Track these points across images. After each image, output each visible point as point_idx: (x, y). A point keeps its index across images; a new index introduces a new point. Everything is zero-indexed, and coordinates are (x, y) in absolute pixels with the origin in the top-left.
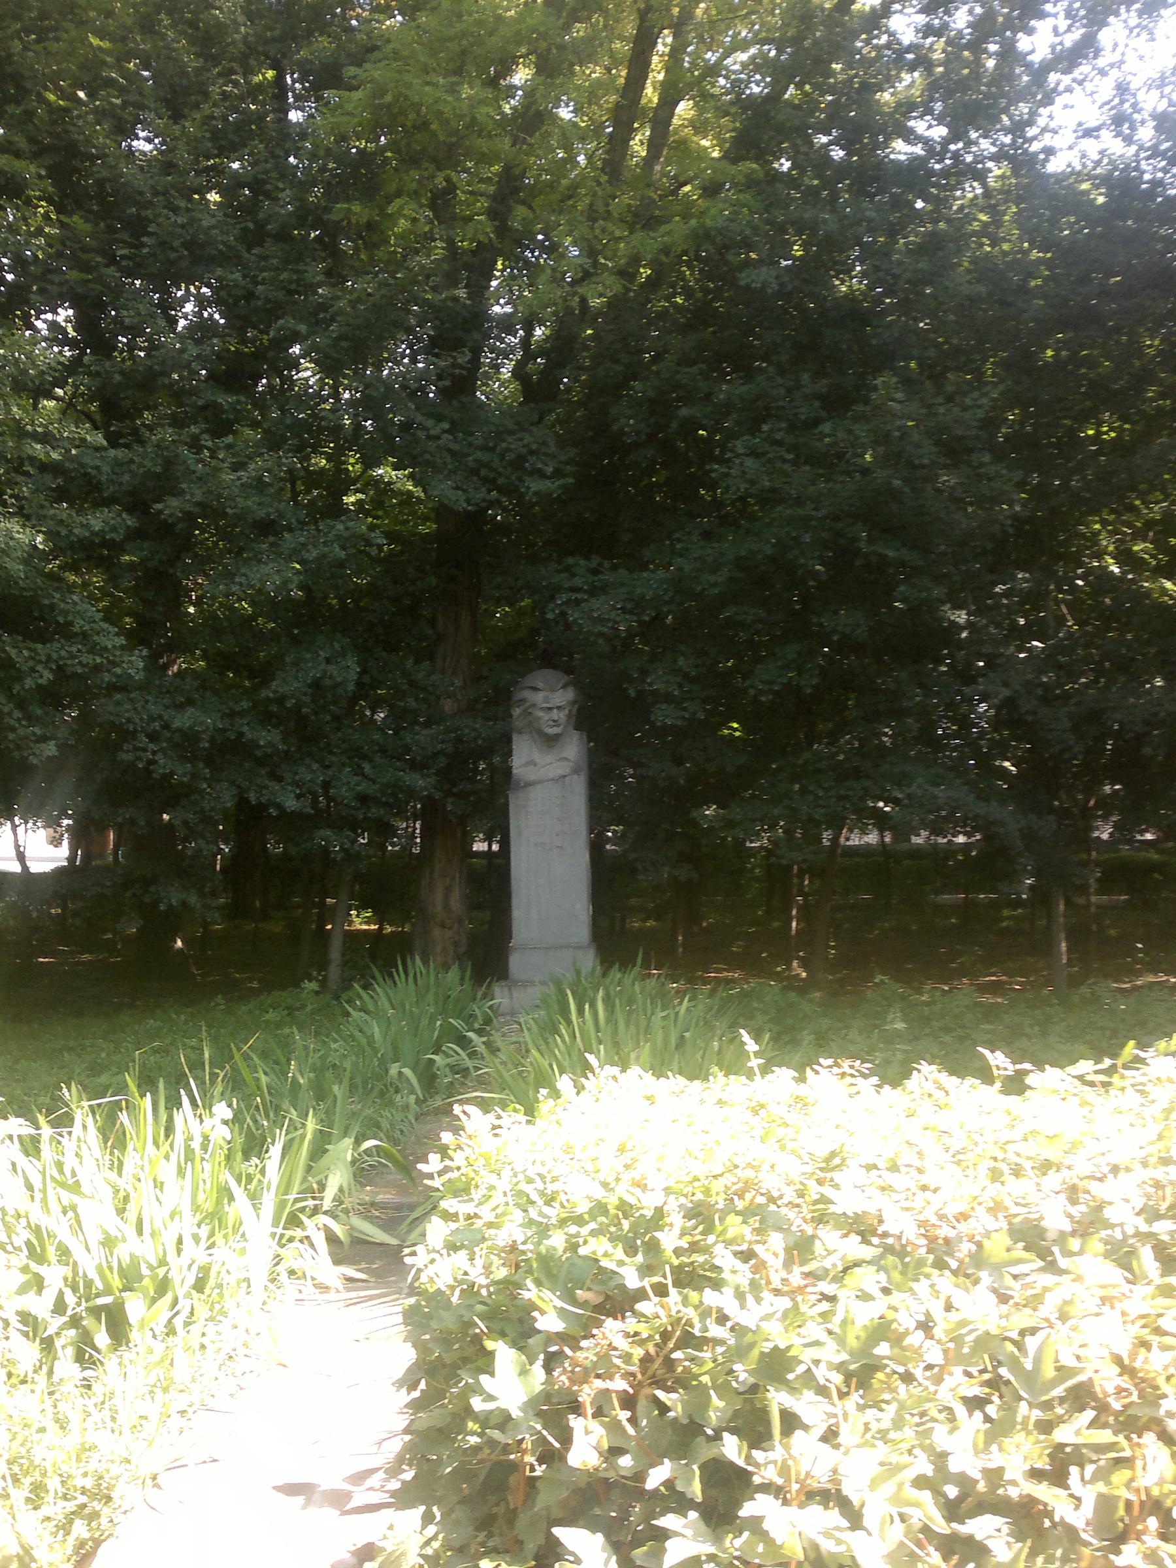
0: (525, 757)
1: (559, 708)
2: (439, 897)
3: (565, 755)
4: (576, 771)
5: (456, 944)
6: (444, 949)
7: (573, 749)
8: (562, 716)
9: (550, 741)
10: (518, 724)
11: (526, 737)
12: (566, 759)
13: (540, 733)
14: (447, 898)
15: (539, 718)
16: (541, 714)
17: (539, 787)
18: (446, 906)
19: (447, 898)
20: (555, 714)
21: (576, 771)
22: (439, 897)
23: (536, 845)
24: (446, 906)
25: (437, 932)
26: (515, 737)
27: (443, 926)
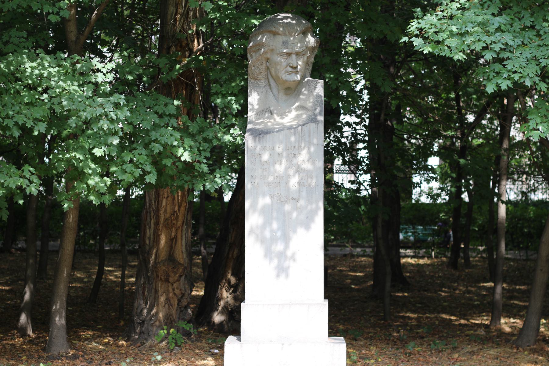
4: (313, 120)
13: (277, 79)
15: (276, 64)
21: (313, 120)
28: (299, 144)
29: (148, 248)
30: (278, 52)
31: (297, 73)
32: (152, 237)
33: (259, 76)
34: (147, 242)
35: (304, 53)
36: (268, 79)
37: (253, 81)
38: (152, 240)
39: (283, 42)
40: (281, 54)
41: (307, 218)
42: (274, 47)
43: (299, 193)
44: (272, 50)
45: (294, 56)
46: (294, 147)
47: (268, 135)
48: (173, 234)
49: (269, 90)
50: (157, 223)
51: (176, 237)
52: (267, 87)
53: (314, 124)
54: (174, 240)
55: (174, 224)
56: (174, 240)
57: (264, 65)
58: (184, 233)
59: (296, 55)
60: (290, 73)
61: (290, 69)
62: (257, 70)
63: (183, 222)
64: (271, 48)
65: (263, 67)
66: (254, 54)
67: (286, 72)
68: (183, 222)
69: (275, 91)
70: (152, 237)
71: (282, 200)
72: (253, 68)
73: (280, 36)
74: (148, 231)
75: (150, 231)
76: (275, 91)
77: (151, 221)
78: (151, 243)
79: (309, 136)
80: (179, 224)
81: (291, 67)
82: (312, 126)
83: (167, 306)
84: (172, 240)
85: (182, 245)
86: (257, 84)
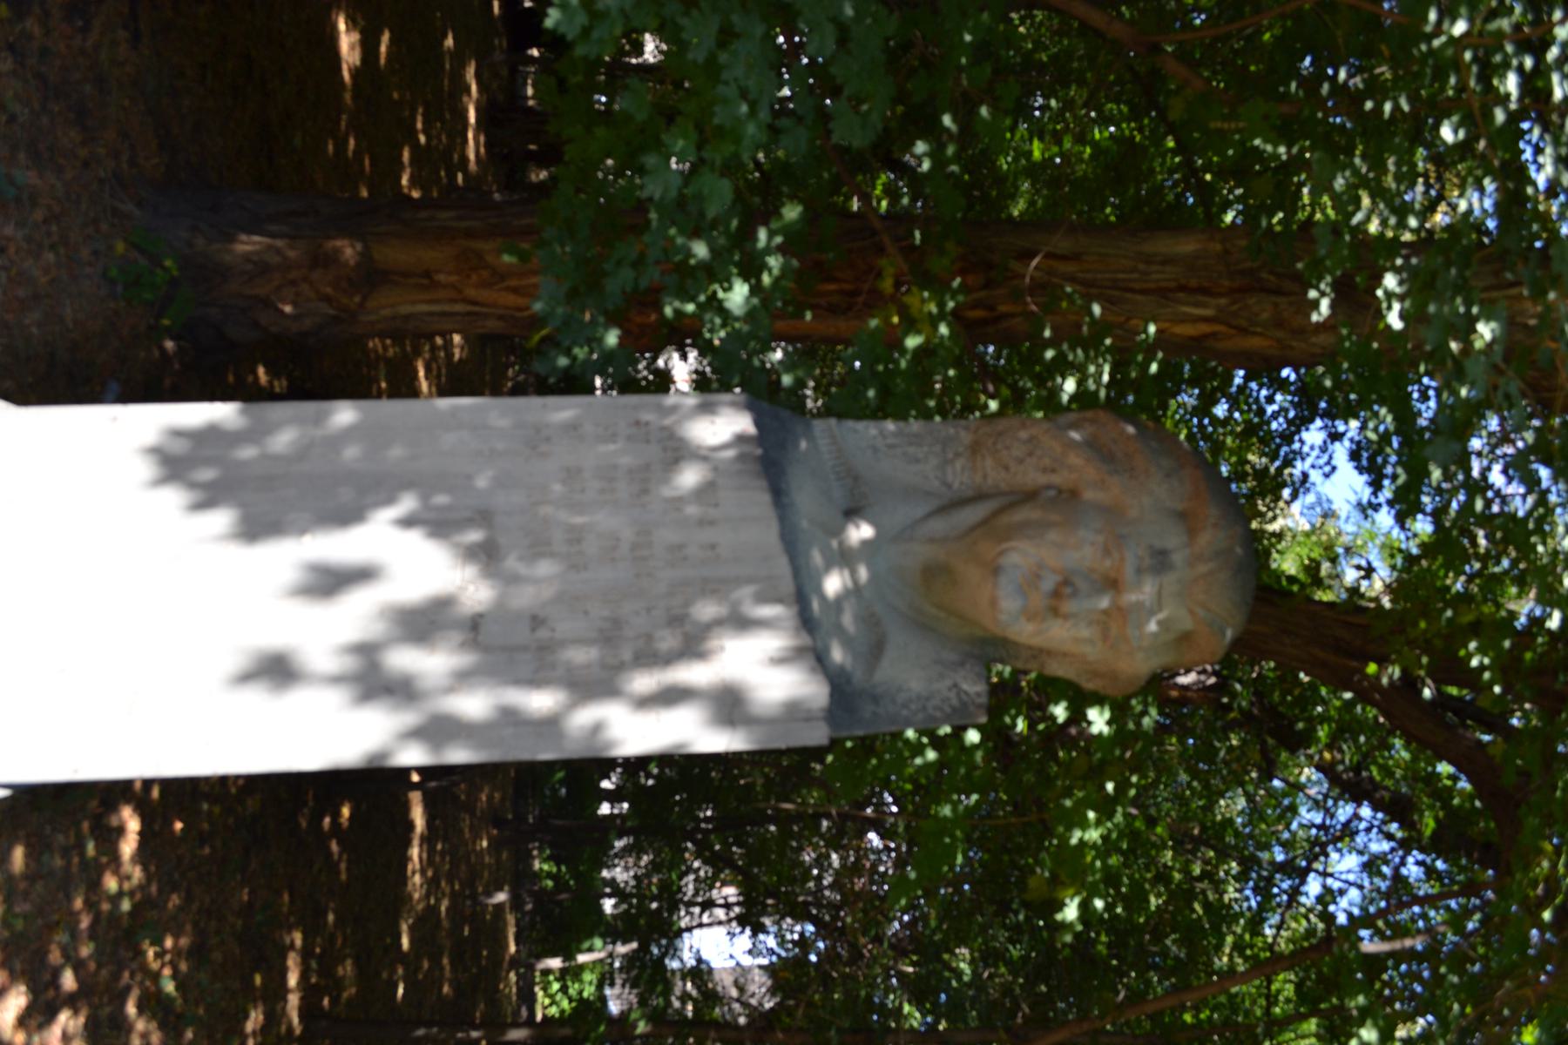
33: (989, 462)
36: (979, 497)
37: (966, 437)
47: (765, 498)
48: (441, 277)
50: (470, 234)
51: (435, 285)
54: (425, 281)
57: (1043, 479)
58: (447, 308)
63: (475, 303)
68: (475, 303)
69: (938, 526)
74: (451, 214)
80: (471, 292)
83: (249, 267)
84: (427, 274)
85: (414, 303)
86: (957, 455)
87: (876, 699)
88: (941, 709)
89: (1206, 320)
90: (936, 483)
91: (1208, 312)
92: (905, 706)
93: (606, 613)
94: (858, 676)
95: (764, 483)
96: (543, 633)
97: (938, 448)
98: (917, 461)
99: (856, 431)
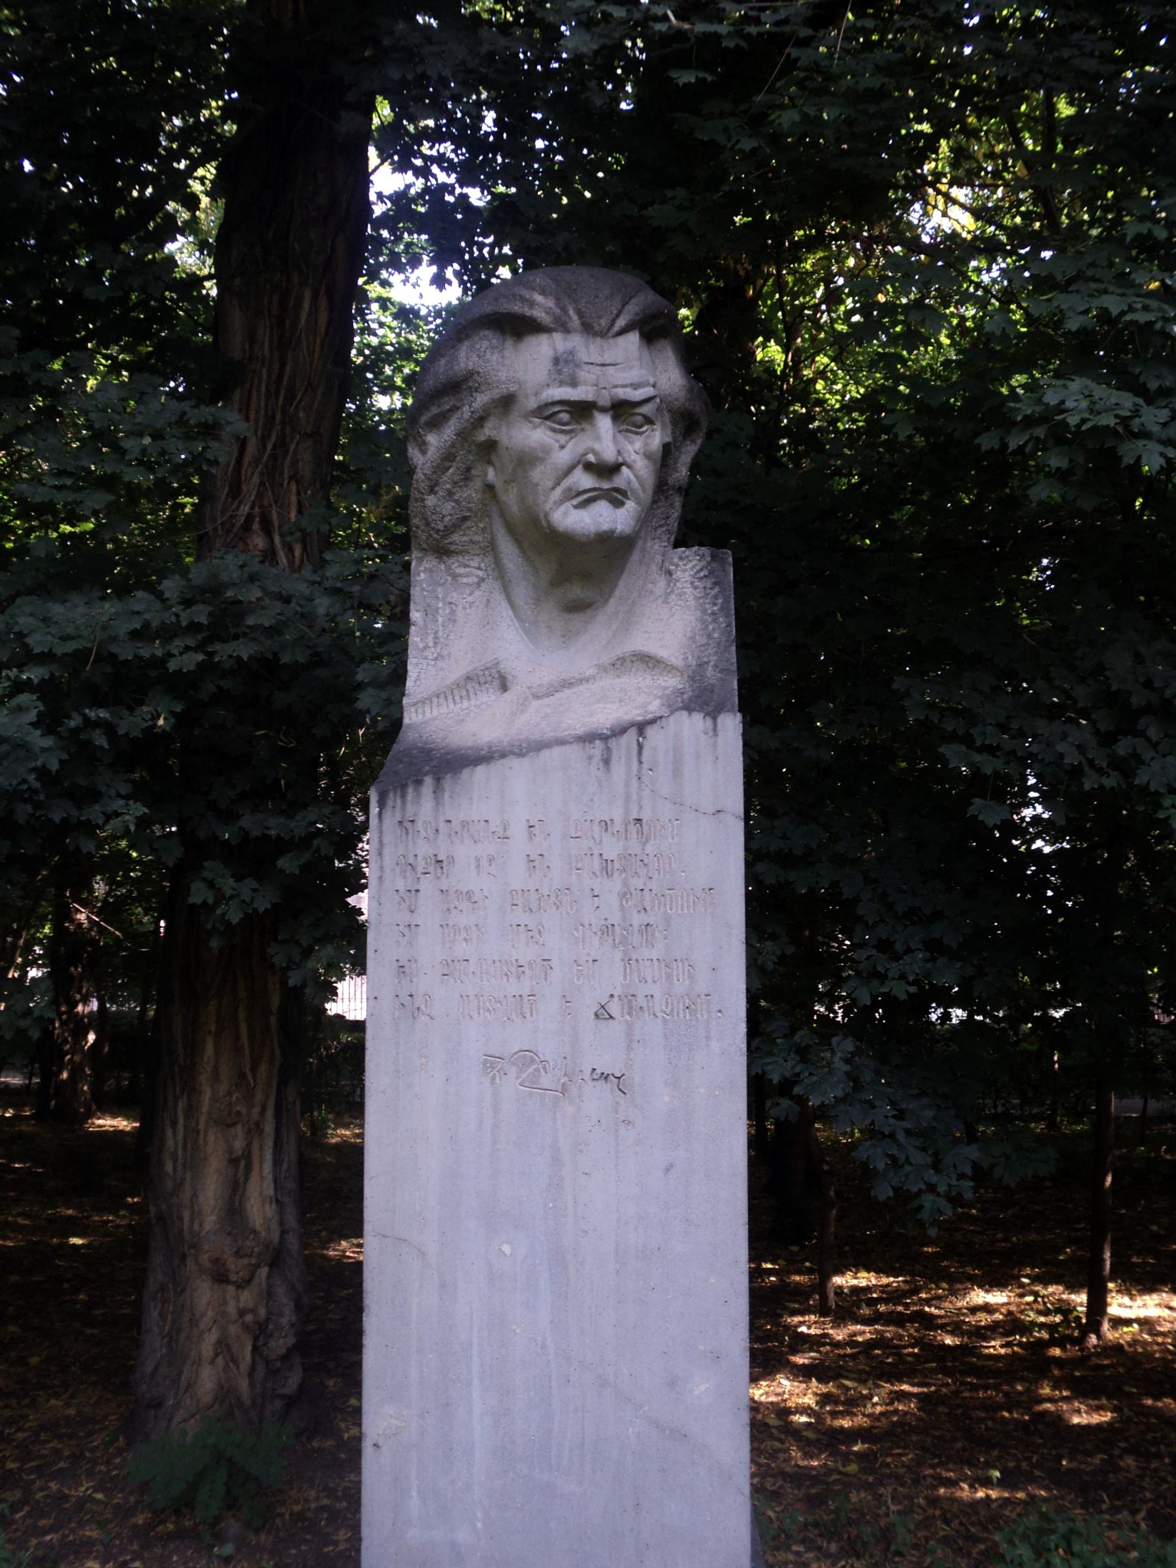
0: (470, 654)
1: (621, 410)
2: (210, 1191)
3: (639, 642)
5: (260, 1332)
6: (223, 1345)
7: (676, 613)
8: (637, 452)
9: (579, 575)
10: (437, 506)
11: (470, 569)
12: (647, 661)
14: (235, 1190)
15: (526, 460)
16: (536, 435)
17: (517, 771)
18: (234, 1210)
19: (235, 1190)
20: (604, 436)
22: (210, 1191)
23: (492, 1064)
24: (234, 1210)
25: (204, 1294)
26: (424, 575)
27: (221, 1277)
28: (627, 810)
29: (169, 1185)
30: (532, 403)
31: (616, 498)
32: (180, 1152)
33: (456, 537)
34: (169, 1167)
35: (646, 409)
36: (491, 548)
38: (180, 1161)
39: (556, 361)
40: (546, 413)
41: (667, 1170)
42: (513, 388)
43: (629, 1048)
44: (507, 403)
45: (604, 422)
46: (606, 825)
47: (480, 769)
48: (239, 1145)
49: (499, 598)
51: (247, 1155)
52: (491, 585)
53: (698, 717)
54: (243, 1163)
55: (239, 1113)
56: (243, 1163)
59: (615, 419)
60: (587, 500)
61: (584, 480)
62: (448, 507)
64: (504, 389)
65: (472, 493)
66: (432, 439)
67: (572, 494)
70: (180, 1152)
71: (546, 1081)
72: (431, 500)
73: (544, 338)
74: (169, 1133)
75: (175, 1133)
76: (522, 592)
77: (176, 1103)
78: (180, 1168)
79: (677, 773)
81: (589, 467)
82: (693, 725)
83: (220, 1361)
84: (234, 1162)
87: (701, 665)
88: (716, 597)
89: (315, 298)
90: (477, 593)
91: (308, 294)
92: (709, 636)
93: (596, 941)
94: (672, 682)
95: (466, 772)
96: (614, 1008)
97: (440, 592)
98: (453, 612)
99: (418, 679)
